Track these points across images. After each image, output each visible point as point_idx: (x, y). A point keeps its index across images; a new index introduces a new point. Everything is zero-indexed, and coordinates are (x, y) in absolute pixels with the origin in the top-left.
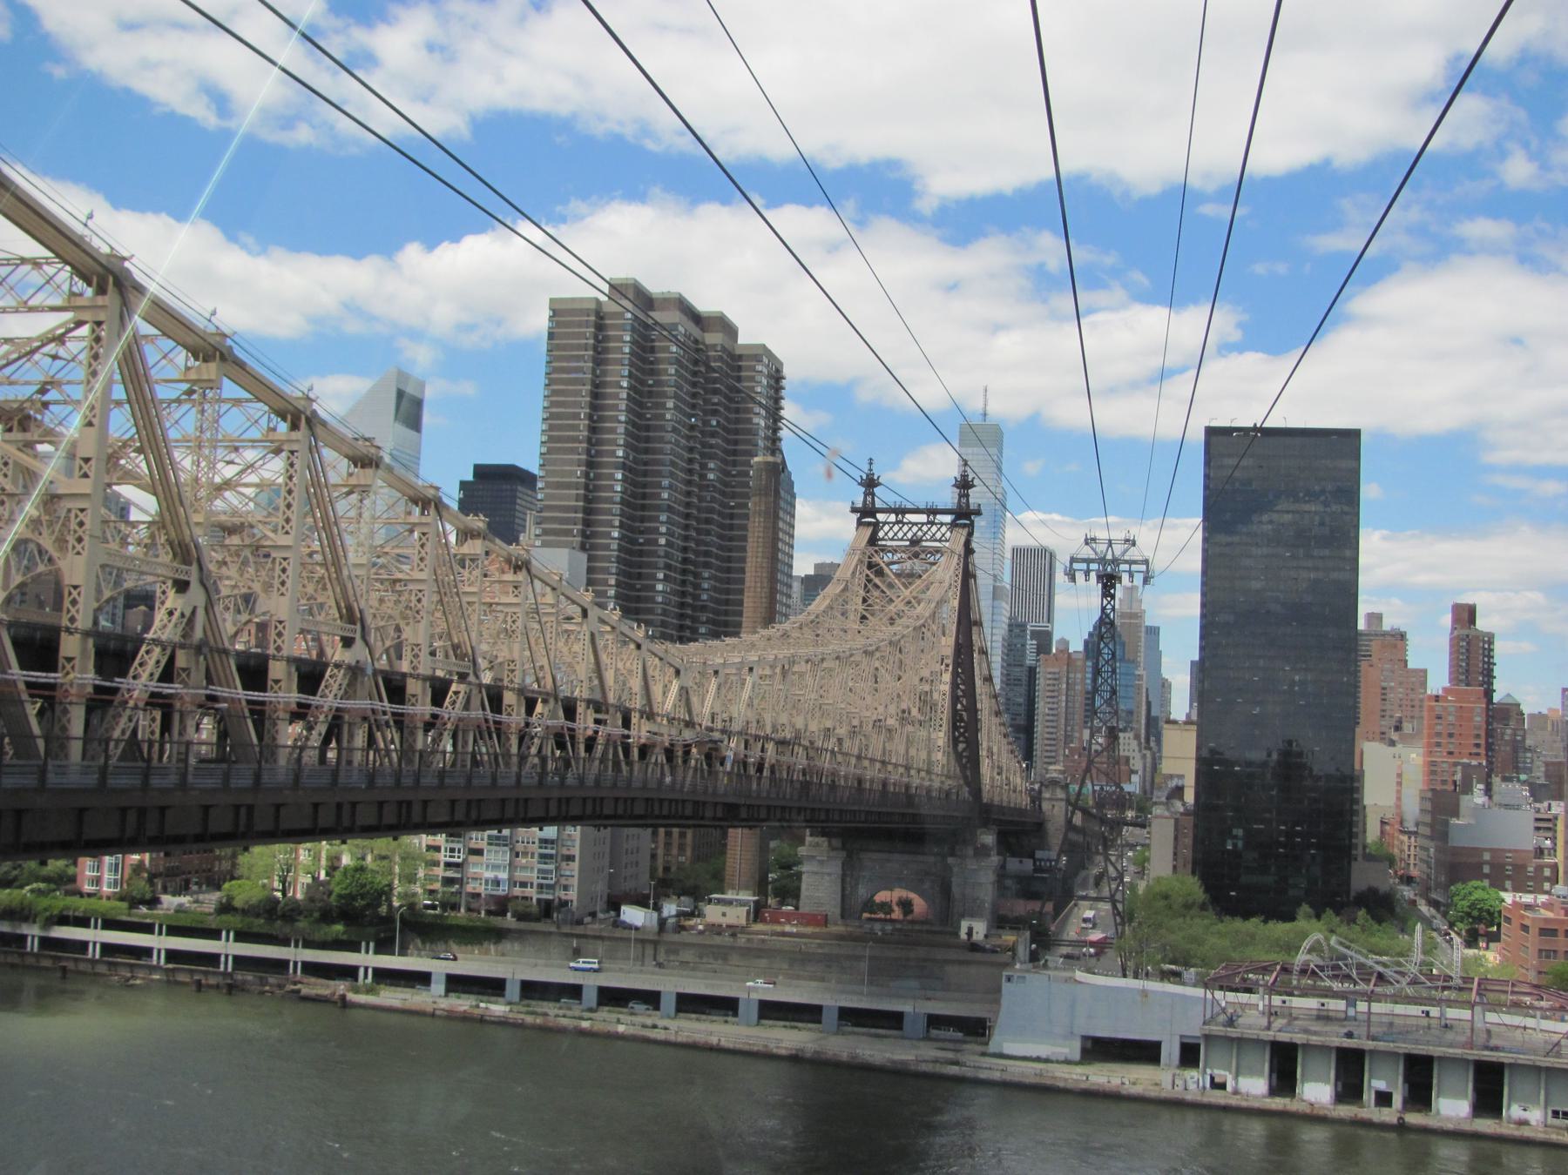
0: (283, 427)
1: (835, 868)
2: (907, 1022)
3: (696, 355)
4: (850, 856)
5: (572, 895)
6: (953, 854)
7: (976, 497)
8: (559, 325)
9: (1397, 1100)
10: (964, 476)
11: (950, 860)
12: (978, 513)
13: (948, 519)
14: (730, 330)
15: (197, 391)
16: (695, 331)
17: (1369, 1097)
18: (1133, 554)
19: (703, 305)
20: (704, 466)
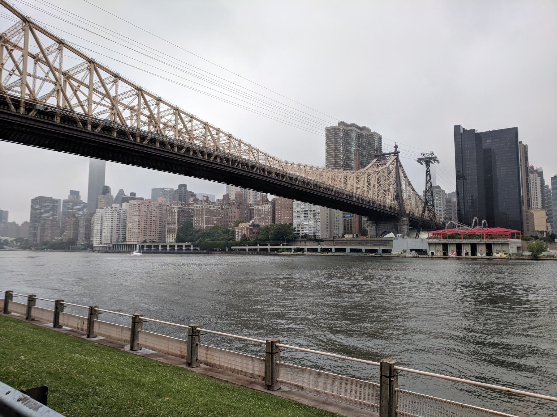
0: (175, 111)
1: (374, 228)
2: (378, 251)
3: (359, 137)
4: (377, 225)
5: (320, 234)
6: (398, 222)
7: (398, 149)
8: (328, 132)
9: (470, 254)
10: (396, 145)
11: (397, 224)
12: (399, 153)
13: (393, 155)
14: (369, 130)
15: (191, 121)
16: (359, 131)
17: (464, 254)
18: (433, 156)
19: (360, 125)
20: (362, 158)
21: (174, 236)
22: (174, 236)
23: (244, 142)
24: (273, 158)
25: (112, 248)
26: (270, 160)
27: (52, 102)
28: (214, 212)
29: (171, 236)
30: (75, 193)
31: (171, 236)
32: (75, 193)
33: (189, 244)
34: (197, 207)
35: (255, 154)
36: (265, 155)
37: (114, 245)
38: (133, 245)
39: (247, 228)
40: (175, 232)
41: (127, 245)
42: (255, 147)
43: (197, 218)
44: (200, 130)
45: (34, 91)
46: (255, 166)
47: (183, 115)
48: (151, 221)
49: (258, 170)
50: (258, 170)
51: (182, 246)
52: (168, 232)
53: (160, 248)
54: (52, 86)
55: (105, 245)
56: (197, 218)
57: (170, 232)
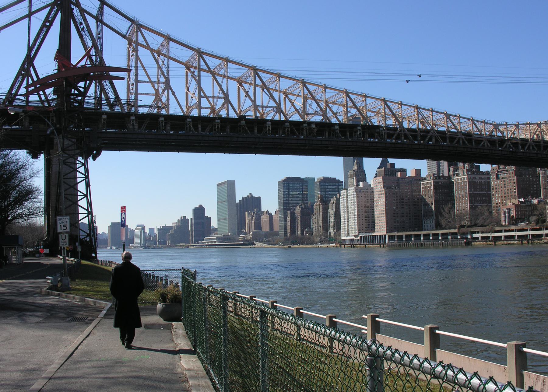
21: (431, 222)
22: (431, 222)
23: (436, 110)
24: (484, 122)
25: (360, 240)
26: (479, 125)
27: (223, 114)
28: (481, 183)
29: (429, 222)
30: (199, 211)
31: (429, 222)
32: (199, 211)
33: (456, 231)
34: (458, 179)
35: (455, 122)
36: (473, 120)
37: (361, 237)
38: (382, 235)
39: (516, 206)
40: (433, 215)
41: (373, 236)
42: (454, 114)
43: (459, 196)
44: (379, 107)
45: (214, 103)
46: (455, 138)
47: (352, 97)
48: (403, 202)
49: (461, 142)
50: (461, 142)
51: (438, 235)
52: (424, 216)
53: (413, 239)
54: (223, 100)
55: (353, 237)
56: (459, 196)
57: (427, 216)
